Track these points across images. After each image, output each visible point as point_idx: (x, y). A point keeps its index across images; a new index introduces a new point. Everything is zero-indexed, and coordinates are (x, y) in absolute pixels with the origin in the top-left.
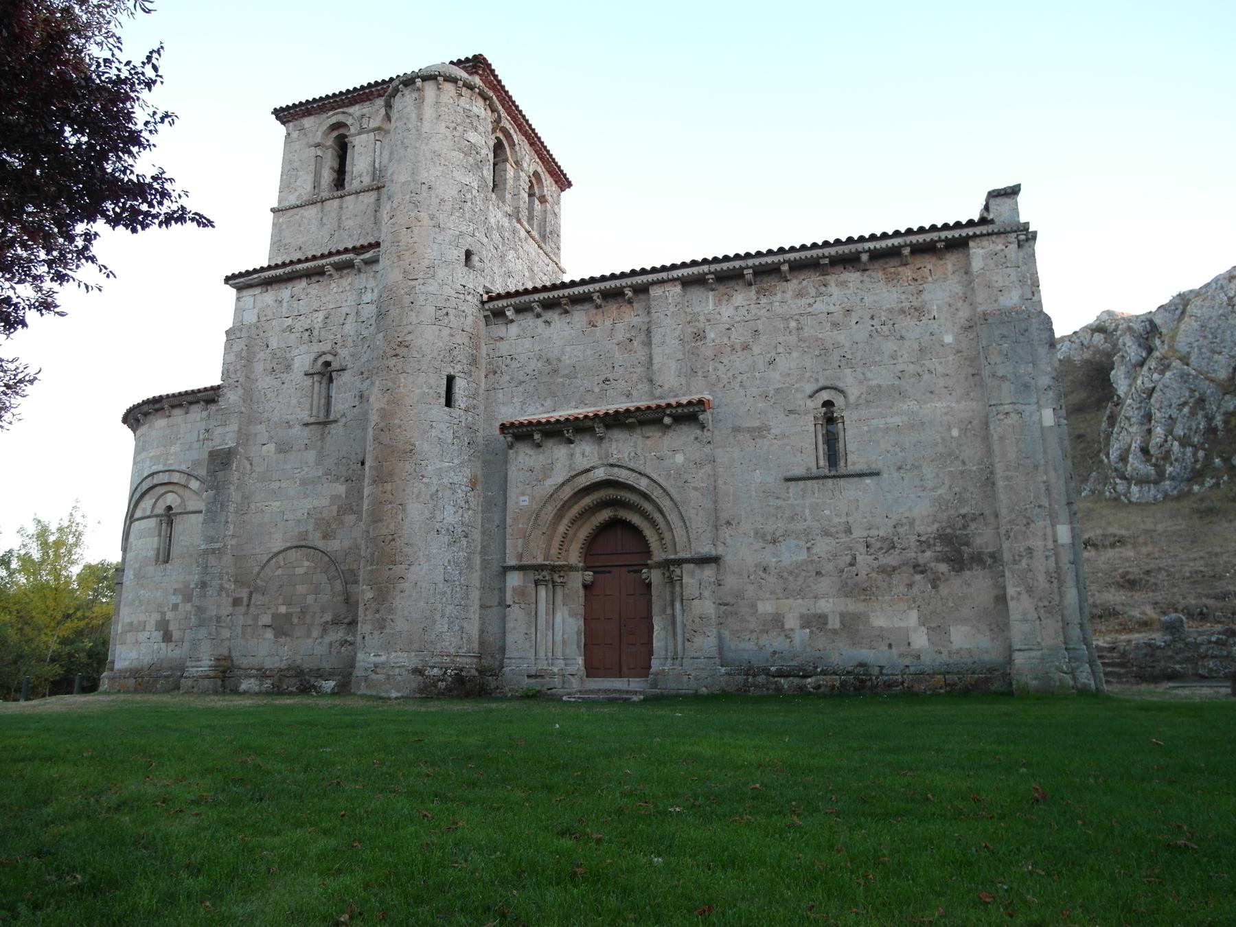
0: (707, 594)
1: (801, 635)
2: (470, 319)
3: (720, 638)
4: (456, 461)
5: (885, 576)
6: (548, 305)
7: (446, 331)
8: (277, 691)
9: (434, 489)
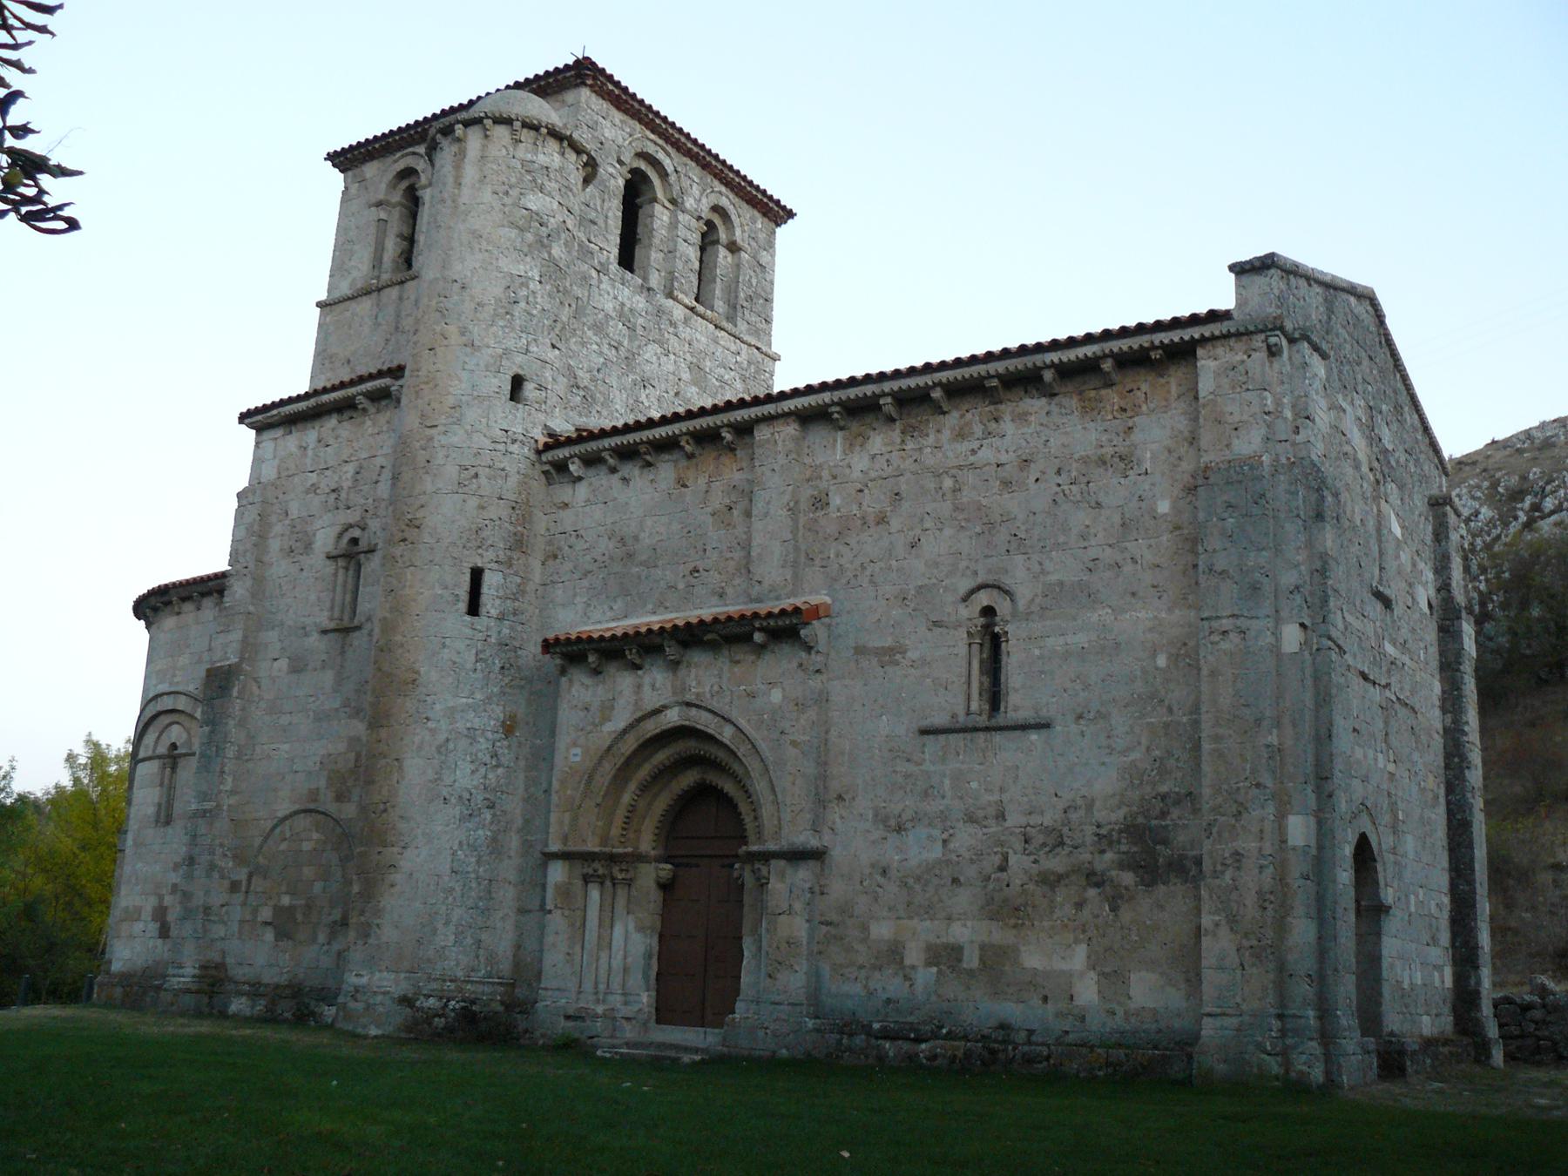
0: (798, 906)
1: (925, 976)
2: (513, 480)
3: (815, 975)
4: (479, 696)
5: (1046, 888)
6: (627, 454)
7: (473, 502)
8: (270, 1019)
9: (442, 737)
